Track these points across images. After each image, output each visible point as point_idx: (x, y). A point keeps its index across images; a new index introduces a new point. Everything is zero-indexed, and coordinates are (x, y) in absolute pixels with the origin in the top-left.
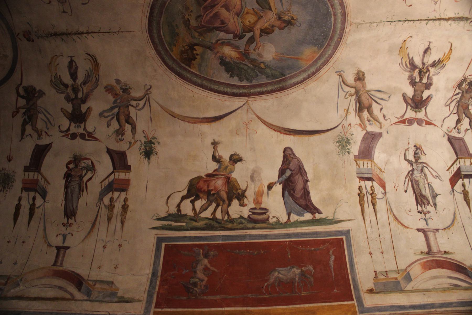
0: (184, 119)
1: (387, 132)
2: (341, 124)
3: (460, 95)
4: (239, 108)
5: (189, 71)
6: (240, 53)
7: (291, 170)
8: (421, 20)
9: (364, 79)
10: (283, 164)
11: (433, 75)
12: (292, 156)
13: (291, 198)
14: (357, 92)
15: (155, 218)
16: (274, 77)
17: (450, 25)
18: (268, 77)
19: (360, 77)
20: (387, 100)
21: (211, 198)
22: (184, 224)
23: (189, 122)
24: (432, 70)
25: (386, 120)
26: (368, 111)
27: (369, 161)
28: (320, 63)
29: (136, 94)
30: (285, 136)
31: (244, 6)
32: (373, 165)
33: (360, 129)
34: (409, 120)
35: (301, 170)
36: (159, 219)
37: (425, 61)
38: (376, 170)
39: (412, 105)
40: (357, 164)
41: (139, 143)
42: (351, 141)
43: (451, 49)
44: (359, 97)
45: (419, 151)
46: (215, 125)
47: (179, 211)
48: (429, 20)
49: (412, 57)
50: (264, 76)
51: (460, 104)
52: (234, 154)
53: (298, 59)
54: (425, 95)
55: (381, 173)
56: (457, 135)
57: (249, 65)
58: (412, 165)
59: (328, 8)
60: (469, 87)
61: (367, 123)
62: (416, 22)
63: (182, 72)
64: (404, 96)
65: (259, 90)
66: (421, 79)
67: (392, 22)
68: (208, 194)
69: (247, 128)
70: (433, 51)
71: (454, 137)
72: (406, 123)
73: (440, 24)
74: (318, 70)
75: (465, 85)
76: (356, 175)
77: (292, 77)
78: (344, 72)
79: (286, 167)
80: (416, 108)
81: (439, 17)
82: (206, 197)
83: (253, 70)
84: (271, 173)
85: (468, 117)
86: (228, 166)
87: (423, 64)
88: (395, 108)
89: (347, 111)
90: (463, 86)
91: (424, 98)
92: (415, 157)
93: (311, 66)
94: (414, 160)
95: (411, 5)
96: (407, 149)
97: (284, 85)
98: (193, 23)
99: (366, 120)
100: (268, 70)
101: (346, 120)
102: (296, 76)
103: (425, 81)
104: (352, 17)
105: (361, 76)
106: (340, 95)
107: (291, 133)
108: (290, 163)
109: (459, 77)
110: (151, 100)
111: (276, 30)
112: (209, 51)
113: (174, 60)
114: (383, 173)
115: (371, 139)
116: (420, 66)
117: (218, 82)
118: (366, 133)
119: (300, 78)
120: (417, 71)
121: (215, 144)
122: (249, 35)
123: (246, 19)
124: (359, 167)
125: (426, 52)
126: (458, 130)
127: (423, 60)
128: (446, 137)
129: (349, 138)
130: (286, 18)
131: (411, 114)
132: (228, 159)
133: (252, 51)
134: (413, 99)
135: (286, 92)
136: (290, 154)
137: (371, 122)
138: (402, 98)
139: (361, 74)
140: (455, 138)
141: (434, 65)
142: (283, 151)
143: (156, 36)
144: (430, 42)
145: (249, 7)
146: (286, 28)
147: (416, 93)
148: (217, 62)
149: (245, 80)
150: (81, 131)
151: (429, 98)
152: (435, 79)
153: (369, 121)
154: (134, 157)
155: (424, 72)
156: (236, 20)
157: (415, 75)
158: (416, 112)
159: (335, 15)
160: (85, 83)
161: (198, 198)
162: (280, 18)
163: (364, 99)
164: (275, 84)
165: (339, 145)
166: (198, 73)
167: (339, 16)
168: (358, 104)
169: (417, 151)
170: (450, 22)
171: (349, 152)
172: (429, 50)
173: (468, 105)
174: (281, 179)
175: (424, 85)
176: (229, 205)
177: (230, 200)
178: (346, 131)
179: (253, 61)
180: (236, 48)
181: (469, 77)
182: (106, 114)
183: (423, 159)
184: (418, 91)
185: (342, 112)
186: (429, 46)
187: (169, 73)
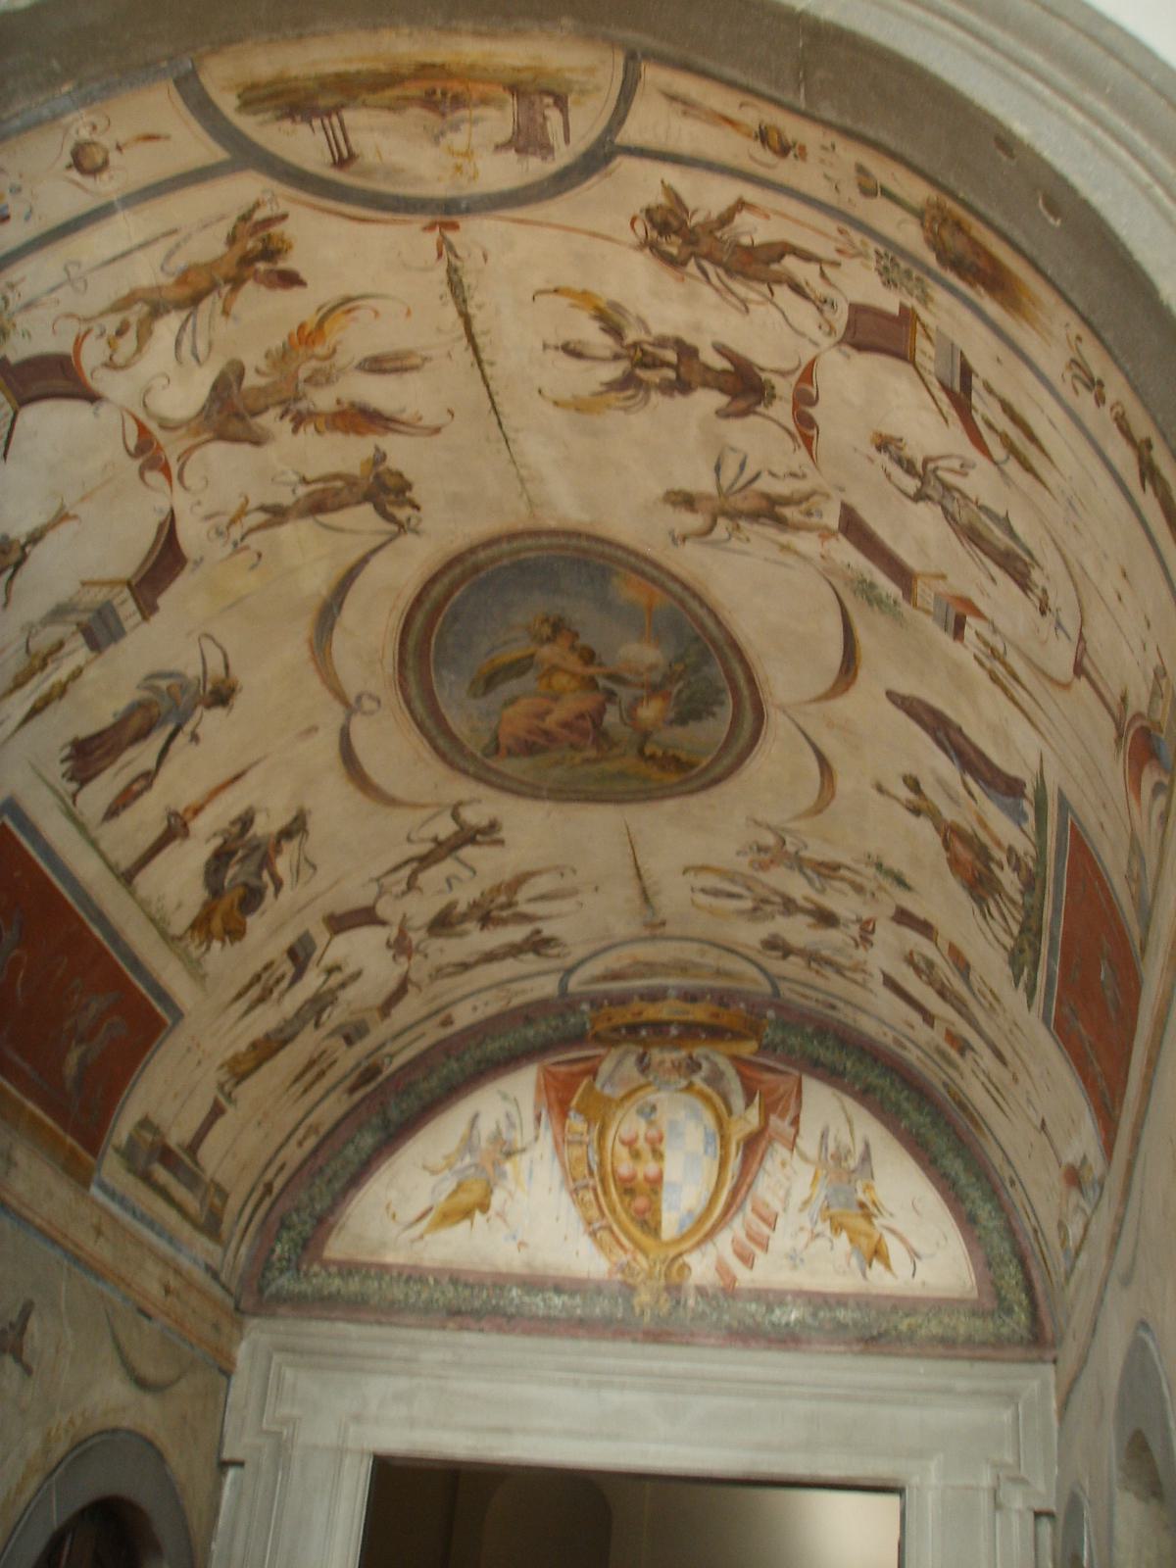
3: (706, 265)
6: (650, 697)
11: (648, 331)
19: (686, 501)
20: (741, 457)
24: (632, 335)
29: (769, 840)
37: (607, 353)
43: (556, 291)
54: (720, 363)
63: (712, 775)
64: (723, 414)
65: (742, 682)
66: (668, 365)
73: (485, 333)
81: (465, 341)
87: (616, 357)
88: (762, 443)
90: (674, 251)
93: (662, 586)
102: (696, 618)
103: (671, 356)
104: (515, 516)
111: (581, 642)
122: (602, 682)
130: (546, 630)
134: (734, 395)
141: (614, 330)
148: (678, 732)
157: (658, 380)
160: (749, 888)
166: (710, 758)
167: (515, 544)
170: (472, 310)
172: (572, 346)
180: (637, 701)
186: (557, 348)
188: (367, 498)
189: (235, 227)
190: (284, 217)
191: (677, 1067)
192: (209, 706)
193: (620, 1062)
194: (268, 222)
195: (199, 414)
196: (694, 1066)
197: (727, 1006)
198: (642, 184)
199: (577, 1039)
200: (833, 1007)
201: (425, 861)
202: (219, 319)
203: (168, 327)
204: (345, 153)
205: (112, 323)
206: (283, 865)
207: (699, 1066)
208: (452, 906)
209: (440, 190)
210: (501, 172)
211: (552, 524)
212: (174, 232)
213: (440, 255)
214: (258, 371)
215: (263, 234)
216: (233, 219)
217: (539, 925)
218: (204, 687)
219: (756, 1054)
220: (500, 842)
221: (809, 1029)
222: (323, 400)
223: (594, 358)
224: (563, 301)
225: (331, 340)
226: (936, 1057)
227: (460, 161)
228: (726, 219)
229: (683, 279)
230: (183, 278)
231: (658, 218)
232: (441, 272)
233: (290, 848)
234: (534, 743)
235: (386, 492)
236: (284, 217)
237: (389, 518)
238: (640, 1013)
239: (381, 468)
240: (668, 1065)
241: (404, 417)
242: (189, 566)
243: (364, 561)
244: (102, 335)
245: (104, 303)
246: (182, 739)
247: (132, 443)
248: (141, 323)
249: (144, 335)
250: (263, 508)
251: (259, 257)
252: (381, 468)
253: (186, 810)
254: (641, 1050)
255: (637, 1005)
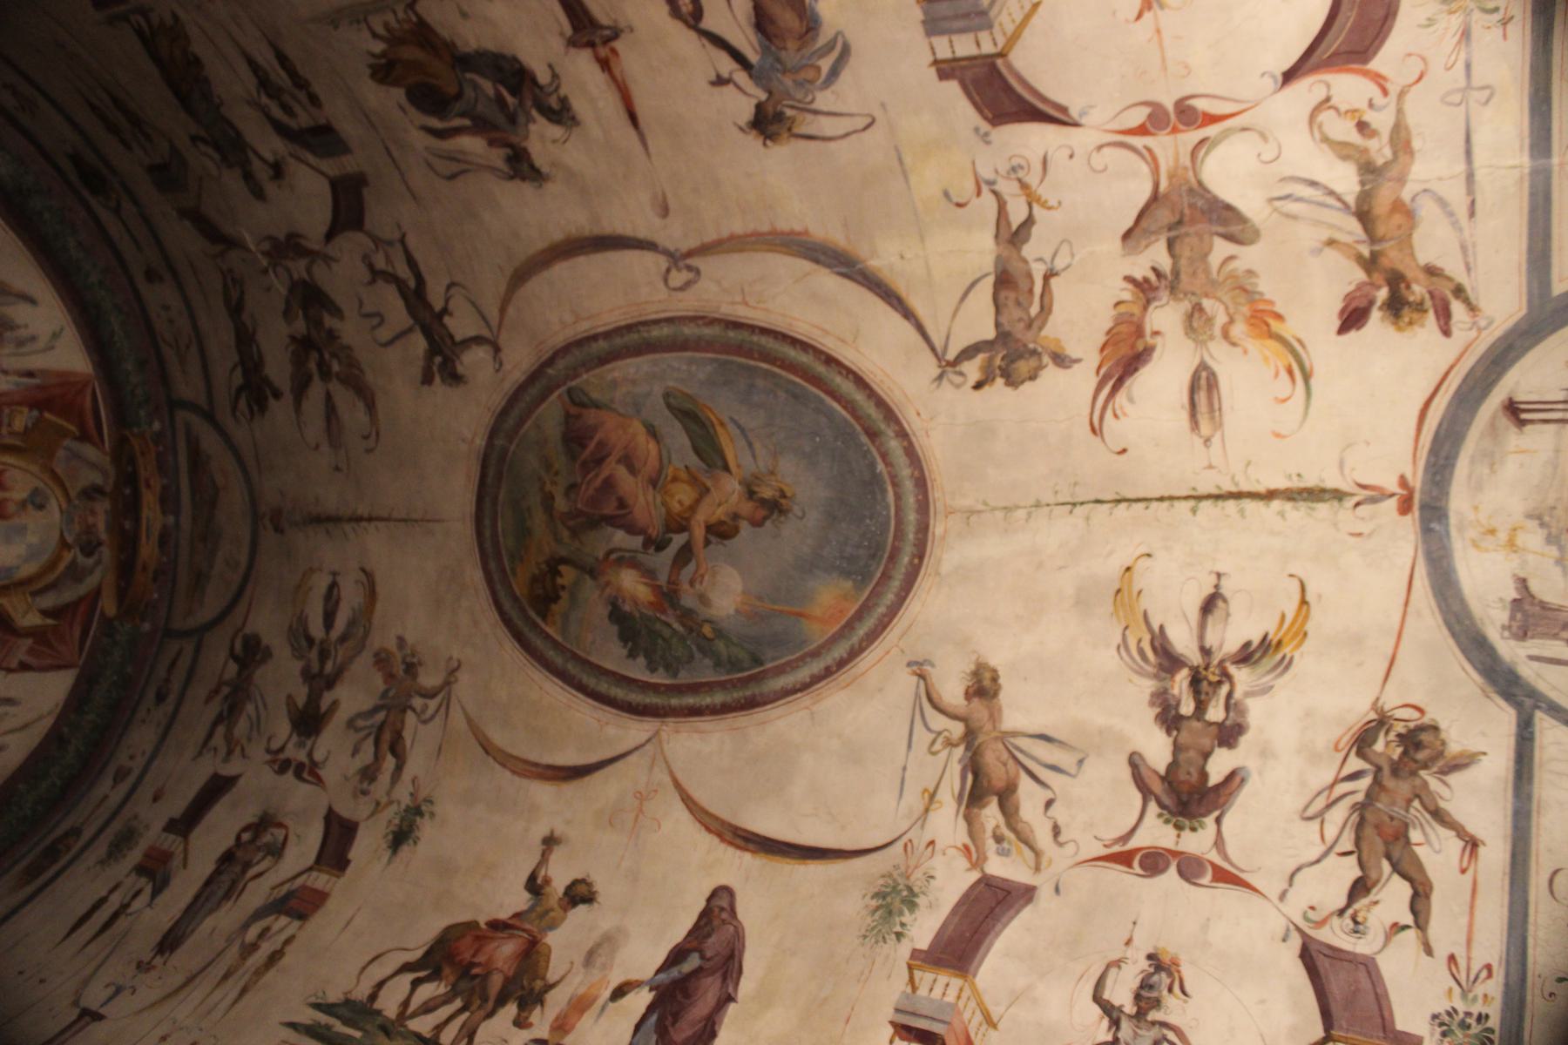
0: (507, 760)
1: (1057, 890)
2: (904, 839)
3: (1364, 783)
4: (636, 748)
5: (543, 631)
6: (656, 589)
7: (702, 957)
8: (1171, 498)
9: (995, 694)
10: (690, 933)
11: (1248, 694)
12: (724, 915)
13: (654, 1037)
14: (970, 735)
15: (313, 1000)
16: (735, 665)
17: (1282, 514)
18: (718, 664)
19: (983, 687)
20: (1073, 771)
21: (463, 985)
22: (358, 1034)
23: (514, 772)
24: (1242, 677)
25: (1061, 845)
26: (1002, 806)
27: (956, 976)
28: (861, 631)
29: (429, 679)
30: (731, 850)
31: (665, 461)
32: (967, 993)
33: (962, 863)
34: (1146, 856)
35: (729, 965)
36: (317, 1006)
37: (1211, 639)
38: (967, 1016)
39: (1167, 801)
40: (912, 980)
41: (394, 808)
42: (921, 900)
43: (1304, 602)
44: (975, 754)
45: (1164, 979)
46: (570, 789)
47: (373, 997)
48: (1199, 498)
49: (1161, 627)
50: (707, 662)
51: (1369, 816)
52: (583, 881)
53: (801, 615)
55: (985, 1026)
56: (1345, 942)
57: (676, 626)
58: (1115, 1024)
59: (873, 465)
60: (1405, 753)
61: (991, 845)
62: (1154, 505)
64: (1136, 764)
65: (690, 700)
66: (1201, 707)
67: (1074, 505)
68: (465, 972)
69: (641, 810)
70: (1236, 605)
71: (1330, 947)
72: (1136, 863)
73: (1242, 512)
74: (854, 654)
75: (1387, 744)
76: (889, 1013)
77: (780, 671)
78: (933, 665)
79: (695, 944)
80: (1182, 814)
81: (1233, 489)
82: (452, 979)
83: (682, 639)
84: (644, 955)
85: (1404, 876)
86: (552, 910)
87: (1206, 652)
89: (932, 796)
90: (1379, 746)
91: (1215, 778)
92: (1138, 997)
94: (1130, 1008)
95: (1124, 451)
96: (1117, 964)
97: (757, 691)
98: (561, 504)
99: (989, 833)
100: (720, 646)
101: (922, 826)
102: (792, 666)
103: (1215, 713)
104: (943, 490)
105: (987, 683)
106: (915, 739)
107: (751, 846)
108: (709, 935)
109: (1359, 710)
110: (453, 698)
111: (745, 527)
112: (589, 582)
113: (515, 599)
114: (992, 1032)
115: (991, 904)
116: (1196, 658)
117: (598, 668)
118: (979, 882)
119: (803, 674)
120: (1182, 678)
121: (550, 842)
122: (678, 540)
123: (672, 496)
124: (914, 989)
125: (1209, 605)
126: (1356, 922)
127: (1201, 637)
128: (1296, 942)
129: (916, 889)
130: (767, 493)
131: (1156, 833)
132: (561, 890)
133: (686, 586)
134: (1169, 777)
135: (759, 715)
136: (722, 909)
137: (1005, 845)
138: (1126, 773)
139: (987, 675)
140: (1336, 954)
141: (1246, 656)
142: (707, 894)
143: (488, 533)
144: (1219, 575)
145: (677, 463)
146: (768, 523)
147: (1182, 757)
148: (602, 611)
149: (661, 670)
150: (302, 756)
151: (1234, 779)
152: (1256, 711)
153: (999, 839)
154: (367, 845)
155: (1210, 683)
156: (650, 498)
157: (1176, 691)
158: (1179, 827)
159: (895, 485)
160: (343, 638)
161: (435, 975)
162: (751, 494)
163: (993, 758)
164: (734, 686)
165: (878, 908)
166: (559, 638)
167: (909, 485)
168: (970, 778)
169: (1155, 978)
170: (1276, 504)
171: (899, 935)
172: (1220, 603)
173: (1406, 826)
174: (662, 976)
175: (1214, 729)
176: (490, 1015)
177: (501, 1001)
178: (912, 863)
179: (687, 615)
180: (649, 574)
181: (1399, 714)
182: (360, 723)
183: (1173, 1010)
184: (1187, 749)
185: (913, 800)
186: (1217, 586)
187: (502, 632)
188: (1003, 336)
189: (1449, 279)
190: (1446, 332)
191: (89, 529)
192: (759, 107)
193: (93, 466)
194: (1444, 315)
195: (1200, 183)
196: (89, 548)
197: (155, 580)
198: (1478, 727)
199: (121, 417)
200: (161, 698)
201: (415, 297)
202: (1326, 234)
203: (1346, 180)
204: (1524, 416)
205: (1382, 120)
206: (472, 144)
207: (89, 554)
208: (337, 312)
209: (1459, 501)
210: (1485, 579)
211: (938, 528)
212: (1472, 214)
213: (1364, 487)
214: (1231, 258)
215: (1428, 303)
216: (1461, 277)
217: (288, 397)
218: (792, 107)
219: (102, 614)
220: (427, 379)
221: (129, 670)
222: (1165, 317)
223: (1202, 626)
224: (1291, 609)
225: (1253, 346)
226: (116, 826)
227: (1503, 536)
228: (1439, 816)
229: (1337, 749)
230: (1405, 212)
231: (1425, 737)
232: (1332, 482)
233: (497, 157)
234: (584, 447)
235: (1010, 356)
236: (1446, 332)
237: (968, 353)
238: (148, 486)
239: (1046, 359)
240: (91, 520)
241: (1121, 398)
242: (985, 126)
243: (908, 314)
244: (1371, 105)
245: (1412, 119)
246: (726, 65)
247: (1201, 105)
248: (1365, 151)
249: (1343, 150)
250: (1029, 222)
251: (1391, 291)
252: (1046, 359)
253: (614, 51)
254: (108, 489)
255: (157, 483)
